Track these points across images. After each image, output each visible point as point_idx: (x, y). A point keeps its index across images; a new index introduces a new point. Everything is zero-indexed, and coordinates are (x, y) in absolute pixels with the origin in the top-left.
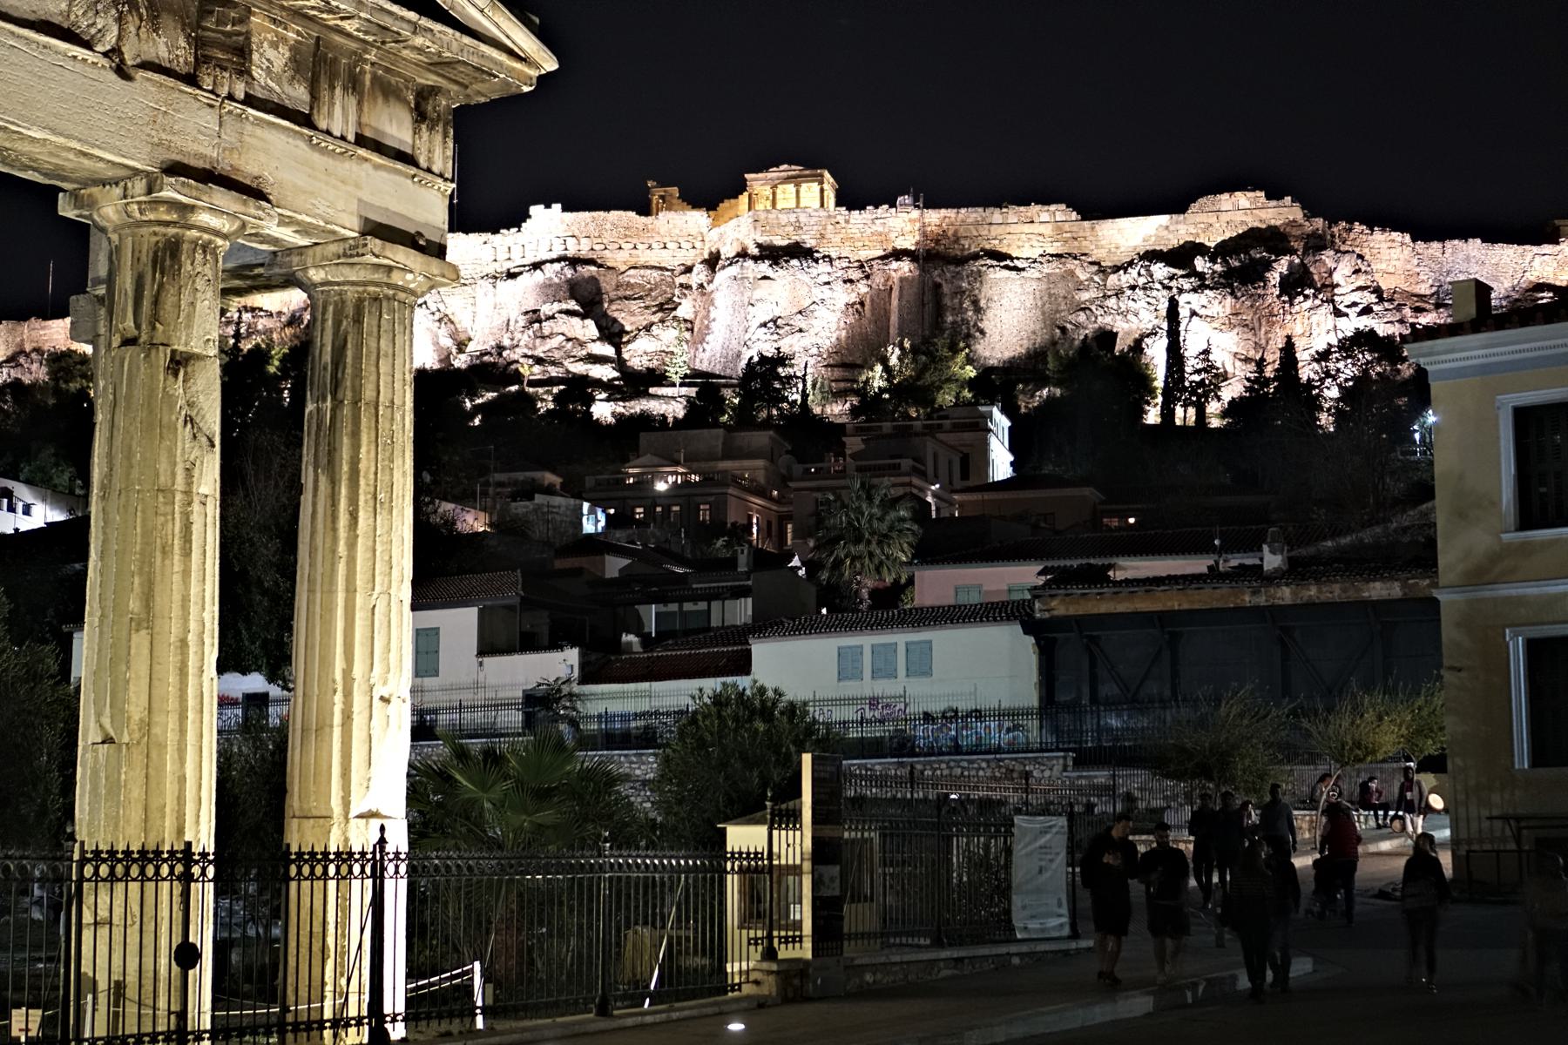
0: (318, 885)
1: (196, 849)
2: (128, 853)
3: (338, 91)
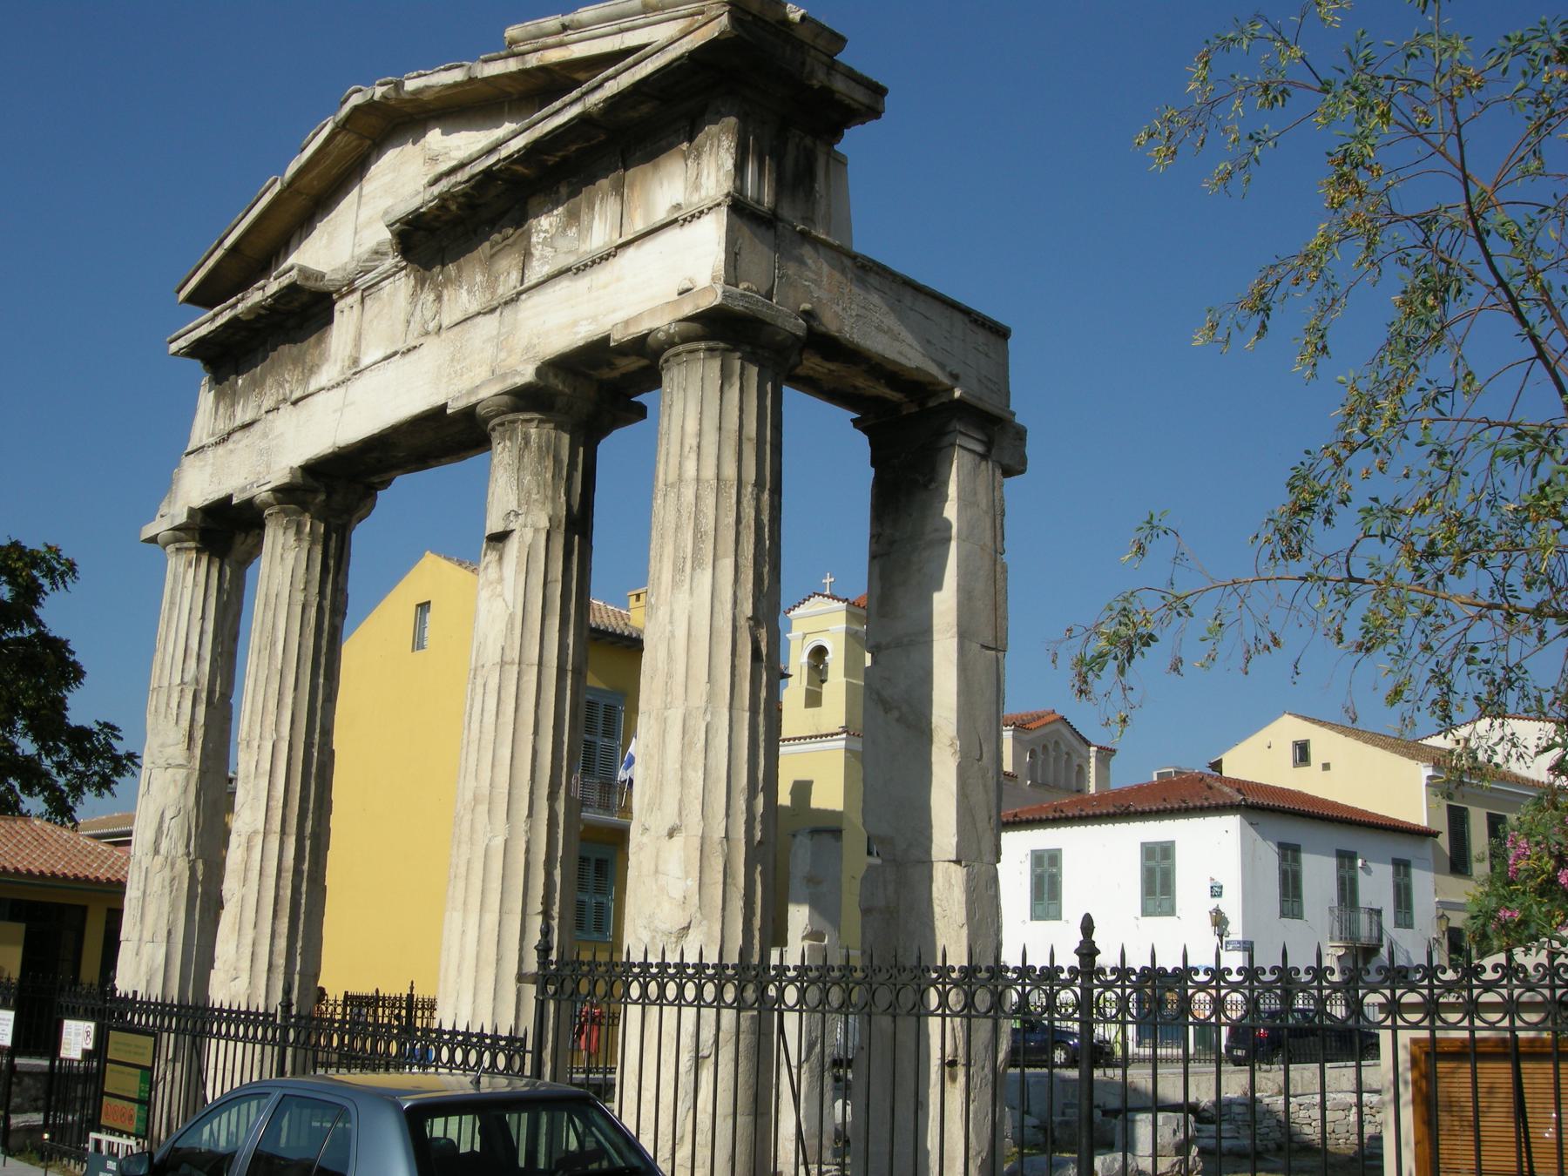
3: (597, 207)
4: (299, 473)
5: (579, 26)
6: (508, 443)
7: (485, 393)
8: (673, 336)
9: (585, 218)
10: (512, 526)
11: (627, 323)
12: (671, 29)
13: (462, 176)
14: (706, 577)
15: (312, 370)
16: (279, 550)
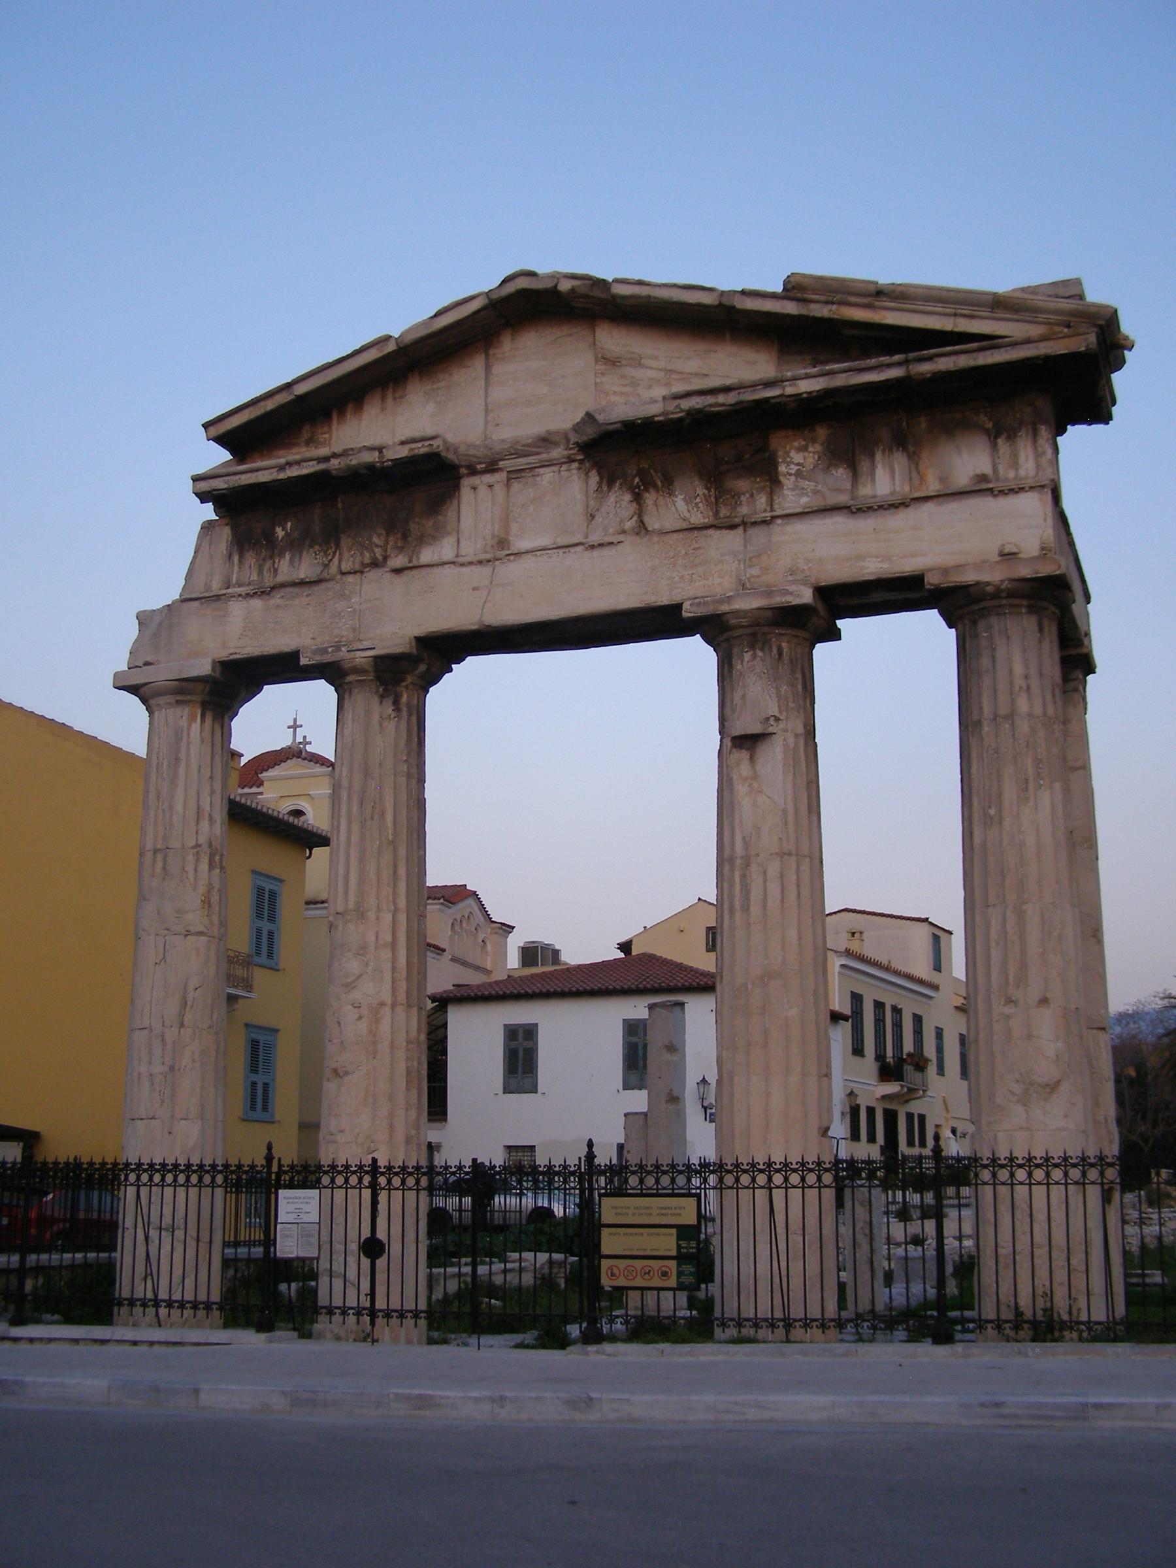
0: (745, 1195)
1: (382, 1163)
2: (214, 1166)
3: (878, 456)
4: (414, 643)
6: (760, 654)
7: (738, 605)
8: (1002, 591)
9: (864, 466)
10: (771, 730)
11: (945, 571)
12: (1035, 331)
13: (721, 399)
14: (1045, 798)
15: (422, 540)
16: (376, 718)
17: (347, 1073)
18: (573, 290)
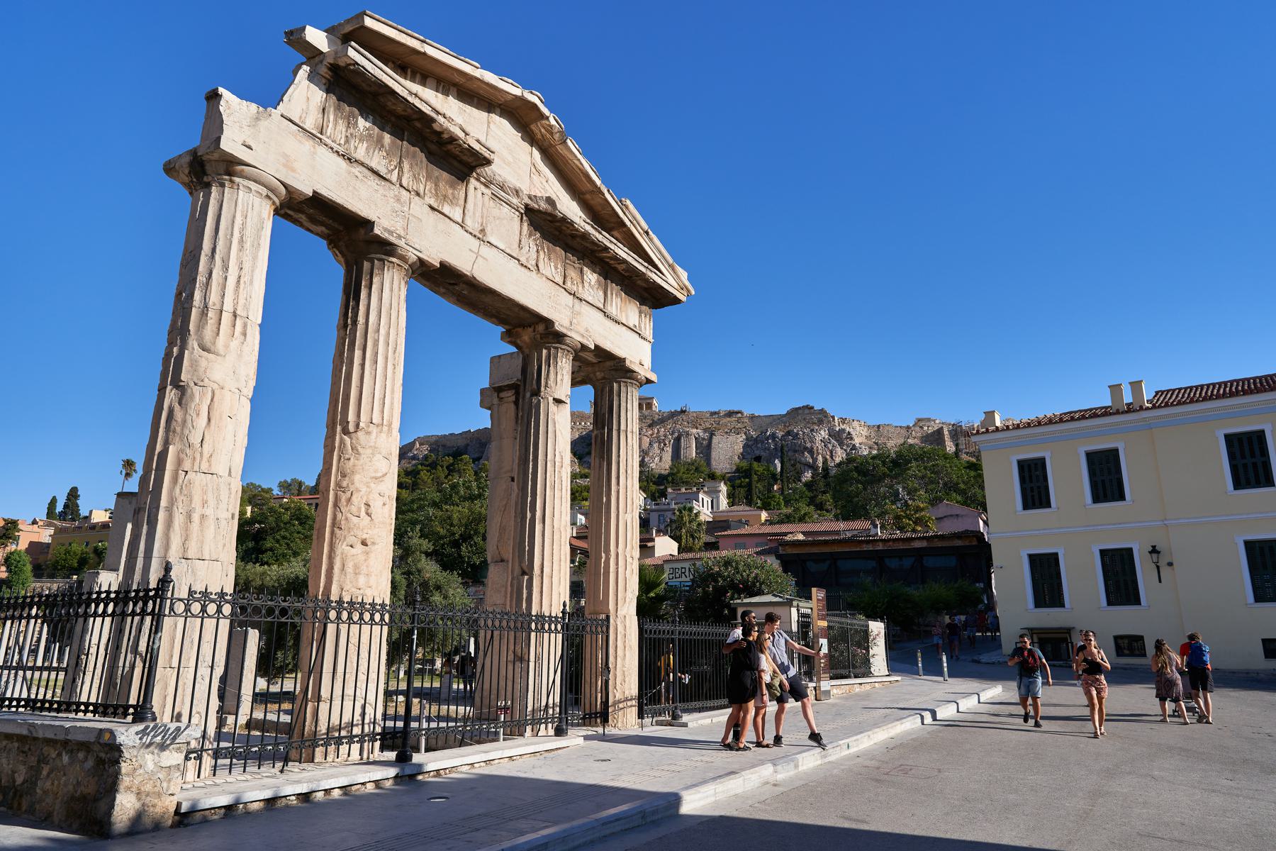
5: (651, 240)
13: (597, 234)
17: (373, 543)
18: (551, 126)
